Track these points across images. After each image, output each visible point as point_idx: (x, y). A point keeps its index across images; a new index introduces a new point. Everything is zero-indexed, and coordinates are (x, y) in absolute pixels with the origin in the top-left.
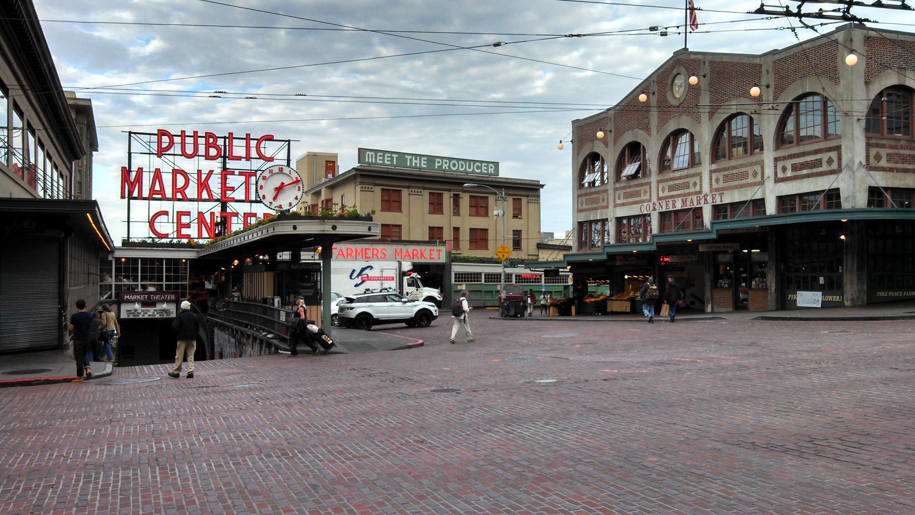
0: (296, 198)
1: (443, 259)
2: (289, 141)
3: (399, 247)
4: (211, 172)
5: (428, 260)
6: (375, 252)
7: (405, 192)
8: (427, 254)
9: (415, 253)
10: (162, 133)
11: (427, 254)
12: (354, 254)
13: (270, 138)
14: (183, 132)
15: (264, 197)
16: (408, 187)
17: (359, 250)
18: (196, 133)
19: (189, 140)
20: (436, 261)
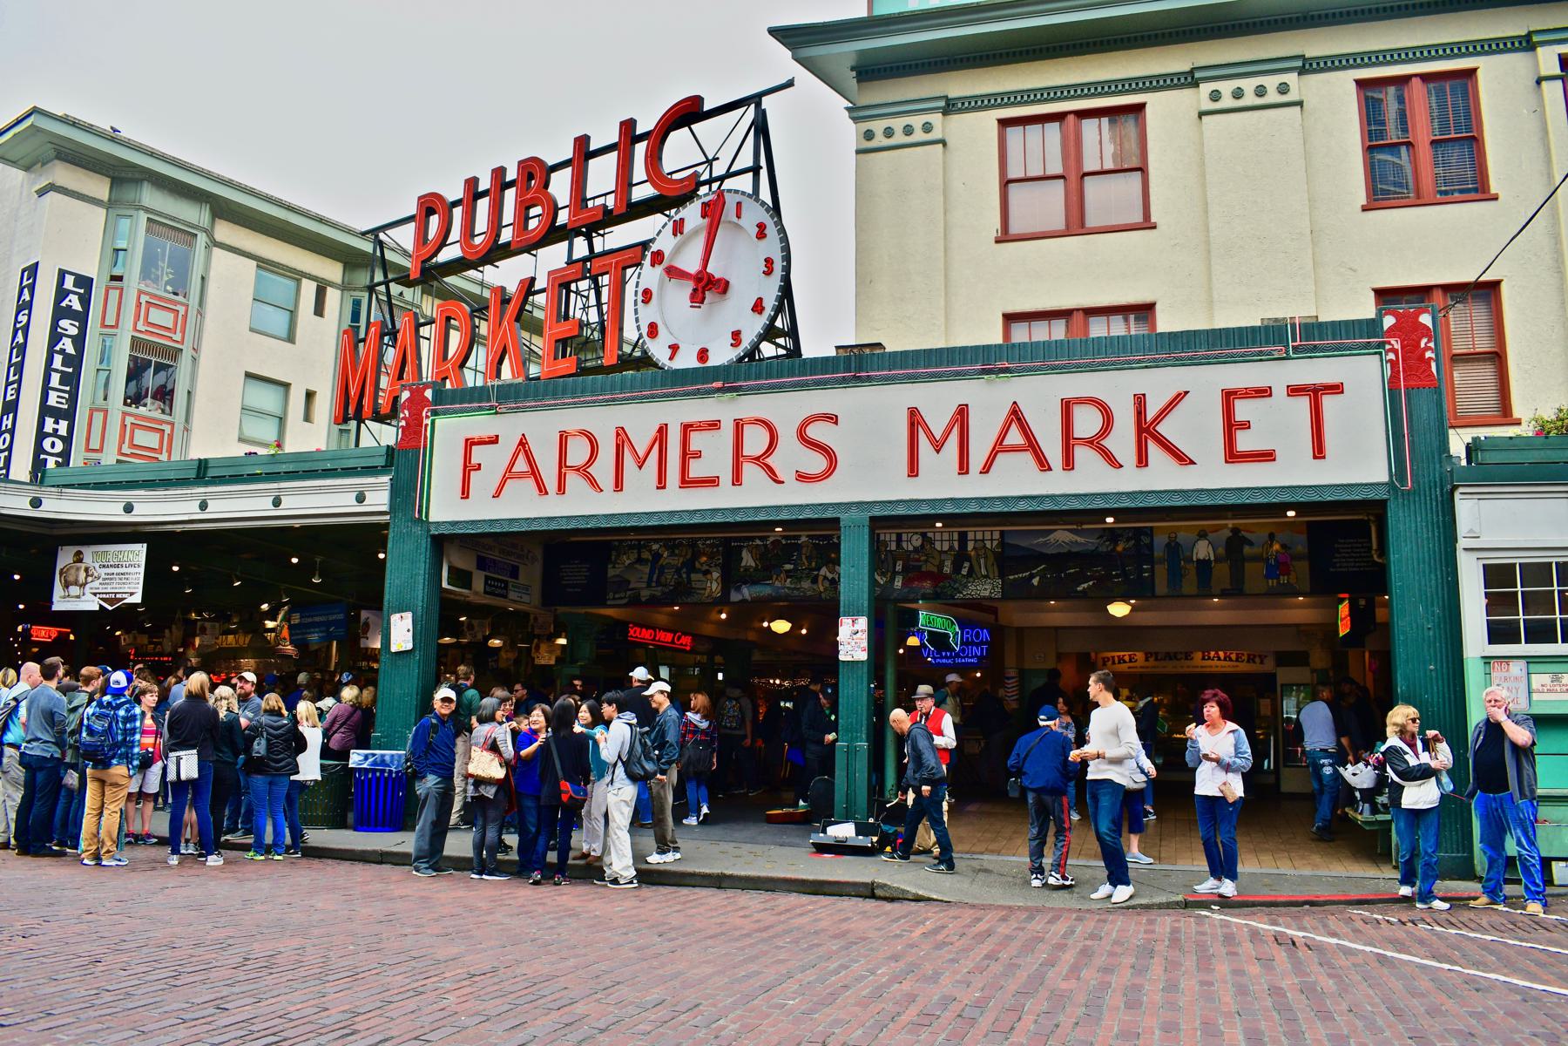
0: (758, 307)
1: (1359, 460)
2: (756, 99)
3: (938, 400)
4: (528, 287)
5: (1212, 475)
6: (755, 441)
7: (1166, 112)
8: (1194, 429)
9: (1087, 422)
10: (430, 205)
11: (1194, 429)
12: (603, 469)
13: (688, 113)
14: (472, 183)
15: (653, 330)
16: (1189, 80)
17: (642, 439)
18: (499, 173)
19: (483, 205)
20: (1294, 472)
